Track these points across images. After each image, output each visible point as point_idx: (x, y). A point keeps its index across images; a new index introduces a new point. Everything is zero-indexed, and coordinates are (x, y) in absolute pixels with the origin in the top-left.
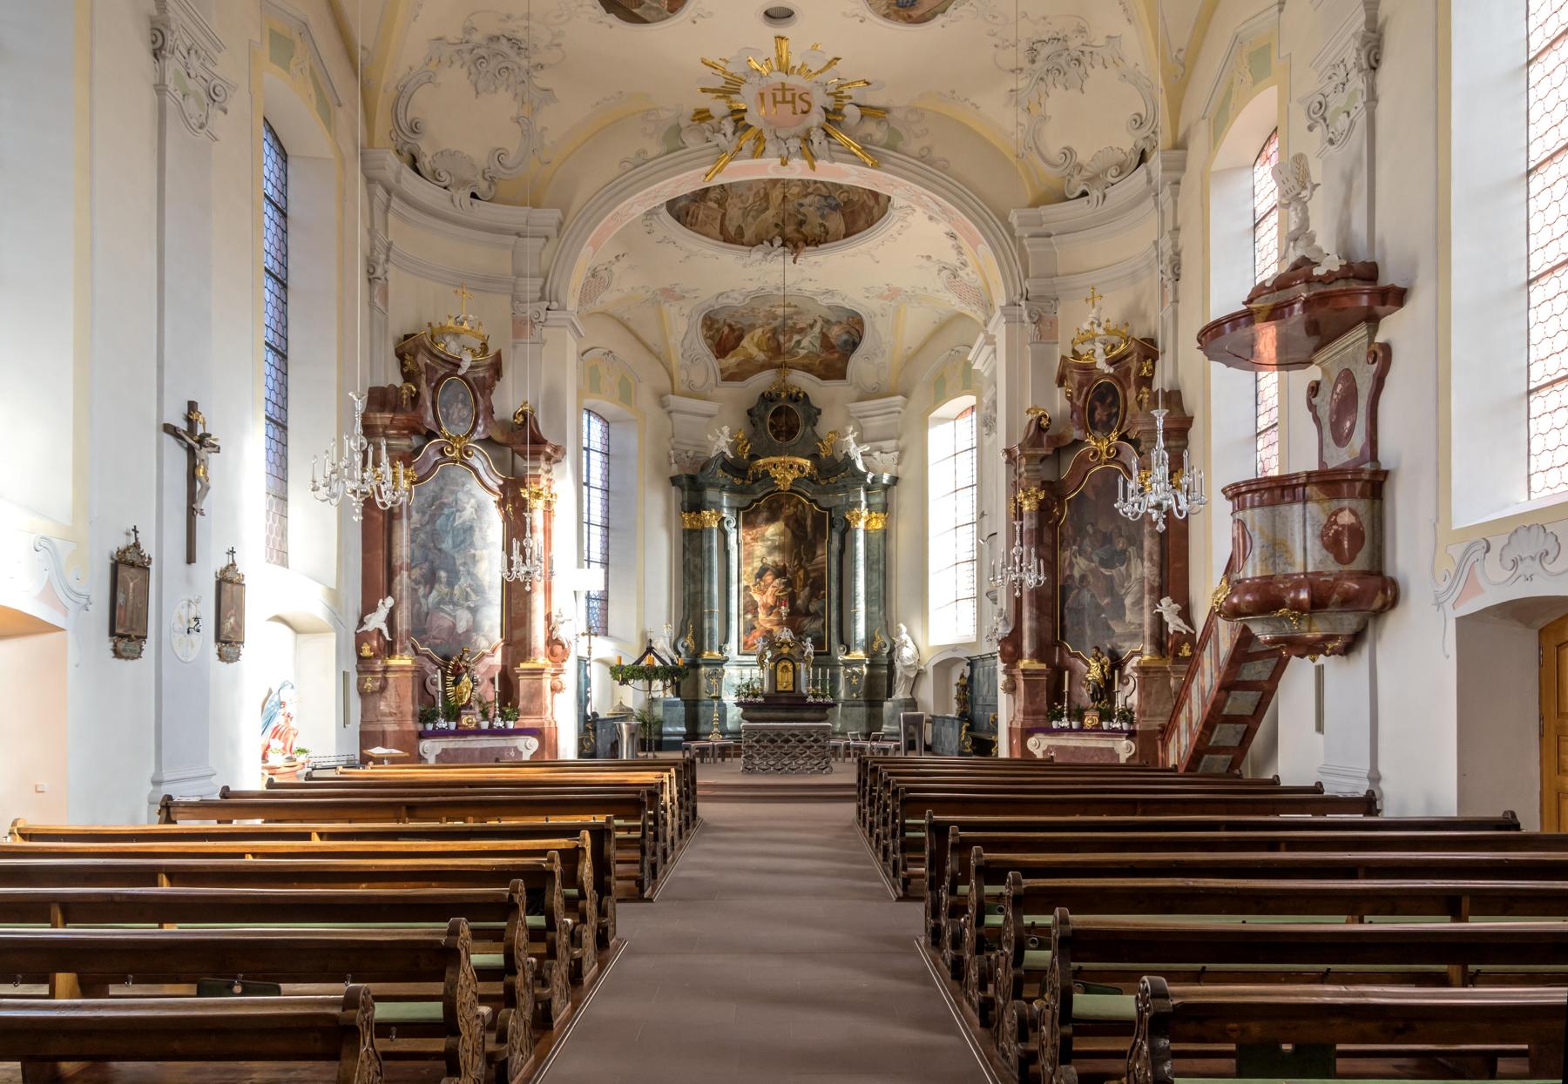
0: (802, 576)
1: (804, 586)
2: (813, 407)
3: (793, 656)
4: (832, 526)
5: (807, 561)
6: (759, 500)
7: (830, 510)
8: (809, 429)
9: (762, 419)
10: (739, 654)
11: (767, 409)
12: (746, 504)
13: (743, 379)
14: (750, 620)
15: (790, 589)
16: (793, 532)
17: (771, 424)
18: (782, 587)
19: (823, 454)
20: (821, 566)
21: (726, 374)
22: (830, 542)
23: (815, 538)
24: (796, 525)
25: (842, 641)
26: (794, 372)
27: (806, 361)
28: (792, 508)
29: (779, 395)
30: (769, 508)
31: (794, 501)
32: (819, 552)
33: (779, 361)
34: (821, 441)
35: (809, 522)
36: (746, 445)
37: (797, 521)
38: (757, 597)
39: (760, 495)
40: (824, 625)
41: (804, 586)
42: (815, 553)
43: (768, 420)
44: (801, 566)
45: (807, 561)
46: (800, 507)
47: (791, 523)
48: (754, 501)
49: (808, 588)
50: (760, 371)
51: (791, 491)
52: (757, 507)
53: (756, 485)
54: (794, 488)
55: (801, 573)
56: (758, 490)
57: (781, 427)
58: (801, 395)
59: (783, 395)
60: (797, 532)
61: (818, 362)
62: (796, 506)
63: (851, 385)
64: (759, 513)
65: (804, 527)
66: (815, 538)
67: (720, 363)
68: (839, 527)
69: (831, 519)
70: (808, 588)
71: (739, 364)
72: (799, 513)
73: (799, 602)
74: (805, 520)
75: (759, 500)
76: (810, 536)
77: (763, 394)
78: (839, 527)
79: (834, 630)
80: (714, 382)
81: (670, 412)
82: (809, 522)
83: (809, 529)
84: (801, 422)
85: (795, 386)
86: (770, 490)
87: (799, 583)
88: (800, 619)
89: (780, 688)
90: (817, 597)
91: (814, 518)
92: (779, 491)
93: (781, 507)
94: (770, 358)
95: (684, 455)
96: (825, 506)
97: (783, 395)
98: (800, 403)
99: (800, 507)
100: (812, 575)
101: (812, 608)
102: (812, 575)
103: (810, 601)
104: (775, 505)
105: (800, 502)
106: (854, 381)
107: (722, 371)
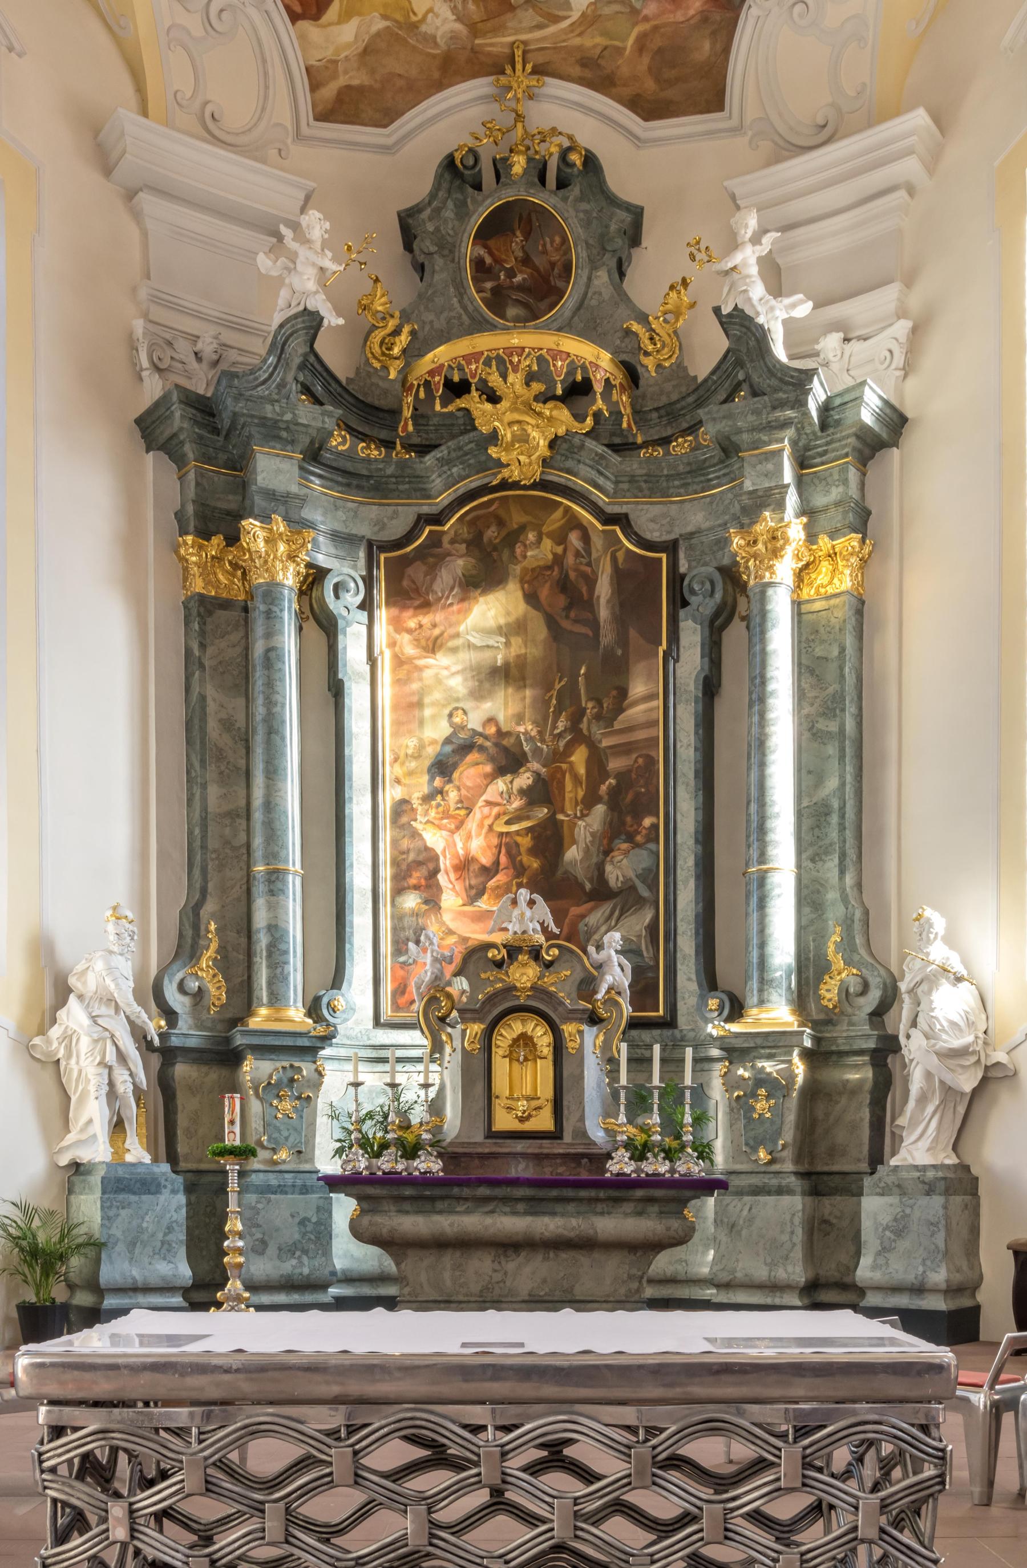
0: (582, 771)
1: (590, 801)
2: (613, 201)
3: (549, 997)
4: (679, 601)
5: (598, 717)
6: (437, 519)
7: (671, 548)
8: (602, 278)
9: (448, 248)
10: (377, 1023)
11: (463, 213)
12: (397, 529)
13: (386, 117)
14: (415, 914)
15: (543, 812)
16: (551, 622)
17: (479, 265)
18: (517, 803)
19: (649, 362)
20: (641, 735)
21: (329, 91)
22: (672, 655)
23: (623, 640)
24: (562, 601)
25: (710, 981)
26: (555, 87)
27: (593, 41)
28: (547, 544)
29: (501, 169)
30: (475, 544)
31: (555, 520)
32: (638, 688)
33: (498, 43)
34: (643, 318)
35: (604, 589)
36: (397, 332)
37: (564, 586)
38: (434, 839)
39: (443, 499)
40: (653, 929)
41: (590, 801)
42: (623, 692)
43: (469, 250)
44: (578, 737)
45: (598, 717)
46: (574, 538)
47: (544, 593)
48: (424, 520)
49: (600, 809)
50: (440, 86)
51: (543, 485)
52: (435, 539)
53: (429, 459)
54: (556, 476)
55: (579, 758)
56: (437, 482)
57: (511, 273)
58: (575, 158)
59: (519, 164)
60: (566, 624)
61: (630, 42)
62: (560, 538)
63: (738, 130)
64: (442, 558)
65: (589, 604)
66: (623, 640)
67: (302, 38)
68: (703, 604)
69: (677, 580)
70: (600, 809)
71: (368, 52)
72: (570, 560)
73: (572, 854)
74: (591, 582)
75: (437, 519)
76: (607, 637)
77: (449, 163)
78: (703, 604)
79: (687, 944)
80: (289, 124)
81: (130, 195)
82: (604, 589)
83: (604, 613)
84: (578, 255)
85: (554, 131)
86: (474, 482)
87: (572, 792)
88: (575, 911)
89: (504, 1121)
90: (630, 838)
91: (620, 576)
92: (504, 485)
93: (513, 538)
94: (474, 29)
95: (184, 349)
96: (654, 534)
97: (519, 164)
98: (575, 191)
99: (574, 538)
100: (615, 764)
101: (615, 874)
102: (615, 764)
103: (607, 852)
104: (491, 533)
105: (574, 523)
106: (751, 113)
107: (315, 78)
